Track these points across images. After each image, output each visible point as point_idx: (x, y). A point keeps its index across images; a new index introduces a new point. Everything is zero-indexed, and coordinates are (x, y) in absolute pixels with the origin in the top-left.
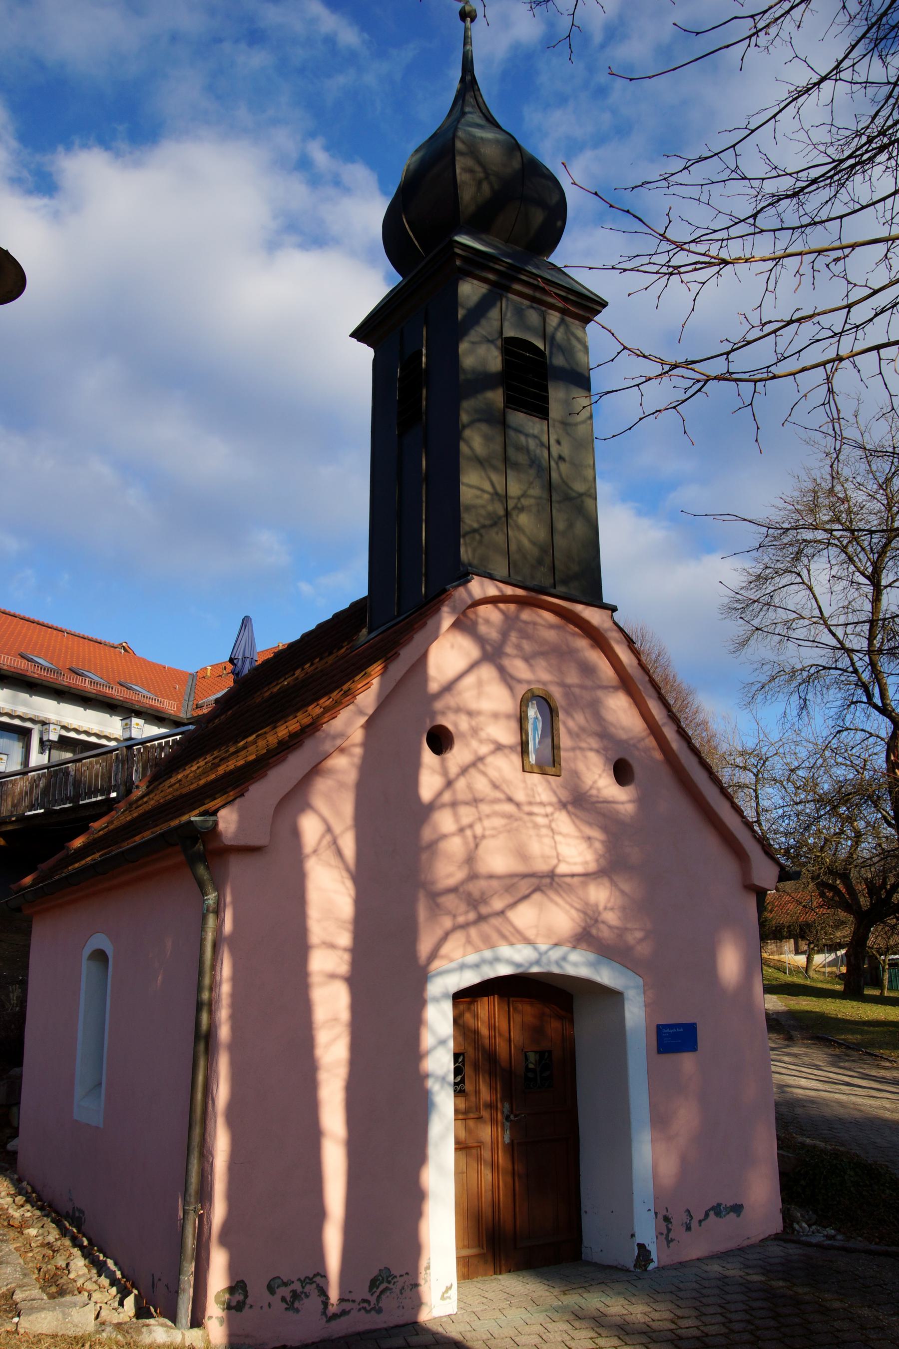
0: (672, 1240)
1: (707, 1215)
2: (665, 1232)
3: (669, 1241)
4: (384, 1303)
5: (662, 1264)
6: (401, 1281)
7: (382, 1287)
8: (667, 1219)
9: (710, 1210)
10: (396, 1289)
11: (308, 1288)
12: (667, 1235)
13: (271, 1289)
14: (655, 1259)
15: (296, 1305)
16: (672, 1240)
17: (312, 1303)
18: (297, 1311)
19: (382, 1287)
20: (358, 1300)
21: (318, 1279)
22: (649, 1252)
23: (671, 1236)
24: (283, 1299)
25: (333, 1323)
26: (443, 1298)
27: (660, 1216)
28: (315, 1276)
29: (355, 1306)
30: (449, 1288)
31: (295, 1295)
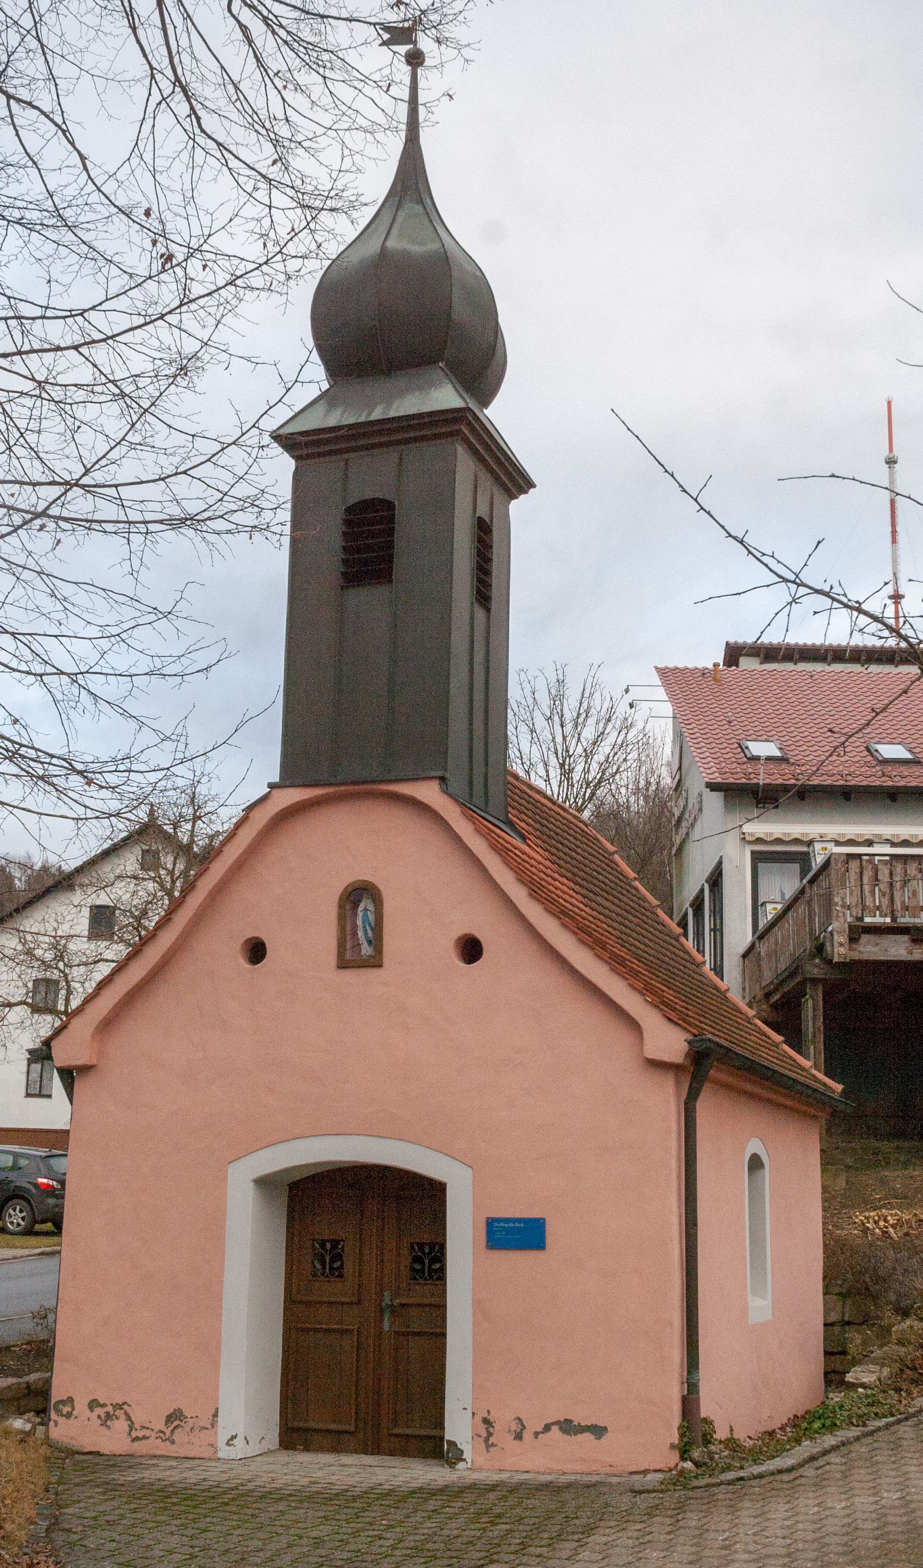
0: (493, 1445)
1: (547, 1428)
2: (484, 1434)
3: (489, 1446)
4: (179, 1436)
5: (477, 1465)
6: (191, 1422)
7: (176, 1423)
8: (486, 1421)
9: (553, 1424)
11: (118, 1412)
12: (486, 1440)
14: (469, 1460)
15: (109, 1423)
16: (493, 1445)
17: (121, 1425)
18: (109, 1427)
19: (176, 1423)
20: (156, 1430)
21: (125, 1407)
22: (462, 1451)
23: (491, 1440)
24: (99, 1417)
25: (136, 1444)
26: (228, 1444)
27: (478, 1418)
28: (125, 1403)
29: (154, 1434)
30: (234, 1437)
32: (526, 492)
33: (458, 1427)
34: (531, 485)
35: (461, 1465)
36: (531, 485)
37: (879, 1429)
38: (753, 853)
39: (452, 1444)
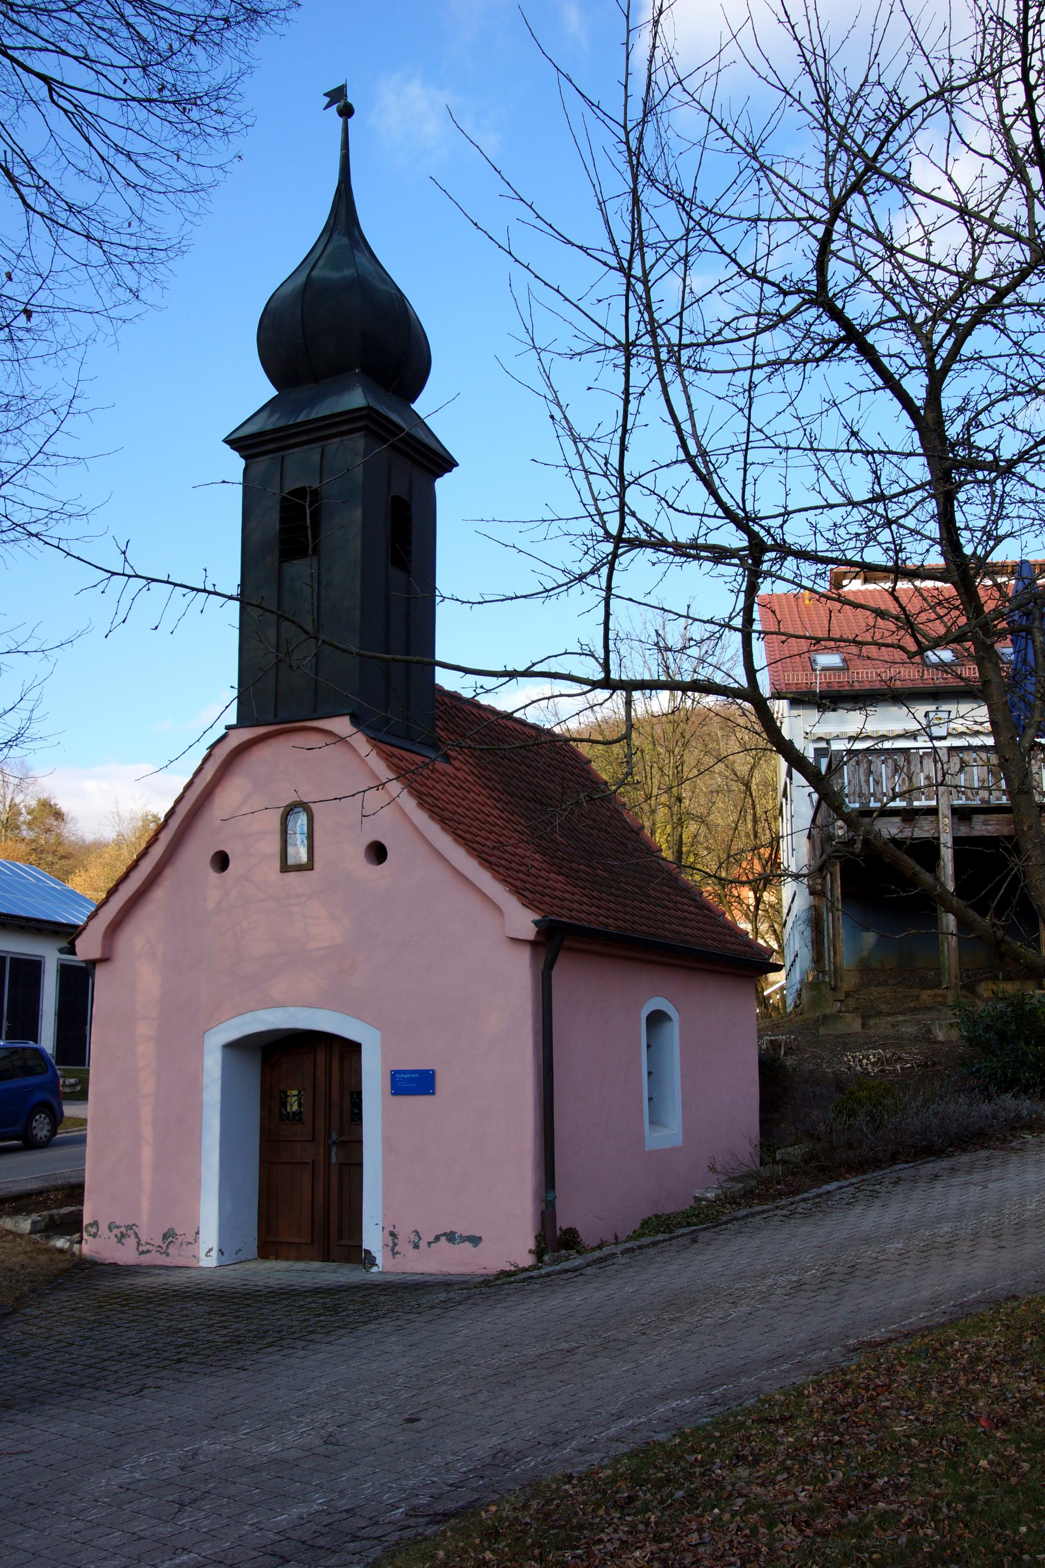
0: (398, 1253)
1: (437, 1238)
2: (391, 1245)
5: (386, 1269)
6: (180, 1238)
10: (178, 1243)
12: (393, 1248)
13: (110, 1229)
14: (380, 1265)
16: (398, 1253)
17: (131, 1241)
18: (123, 1244)
26: (206, 1255)
27: (387, 1231)
29: (154, 1248)
30: (211, 1250)
31: (123, 1235)
32: (450, 471)
33: (372, 1239)
34: (457, 465)
35: (374, 1269)
36: (457, 465)
37: (683, 1235)
38: (816, 750)
39: (368, 1252)
